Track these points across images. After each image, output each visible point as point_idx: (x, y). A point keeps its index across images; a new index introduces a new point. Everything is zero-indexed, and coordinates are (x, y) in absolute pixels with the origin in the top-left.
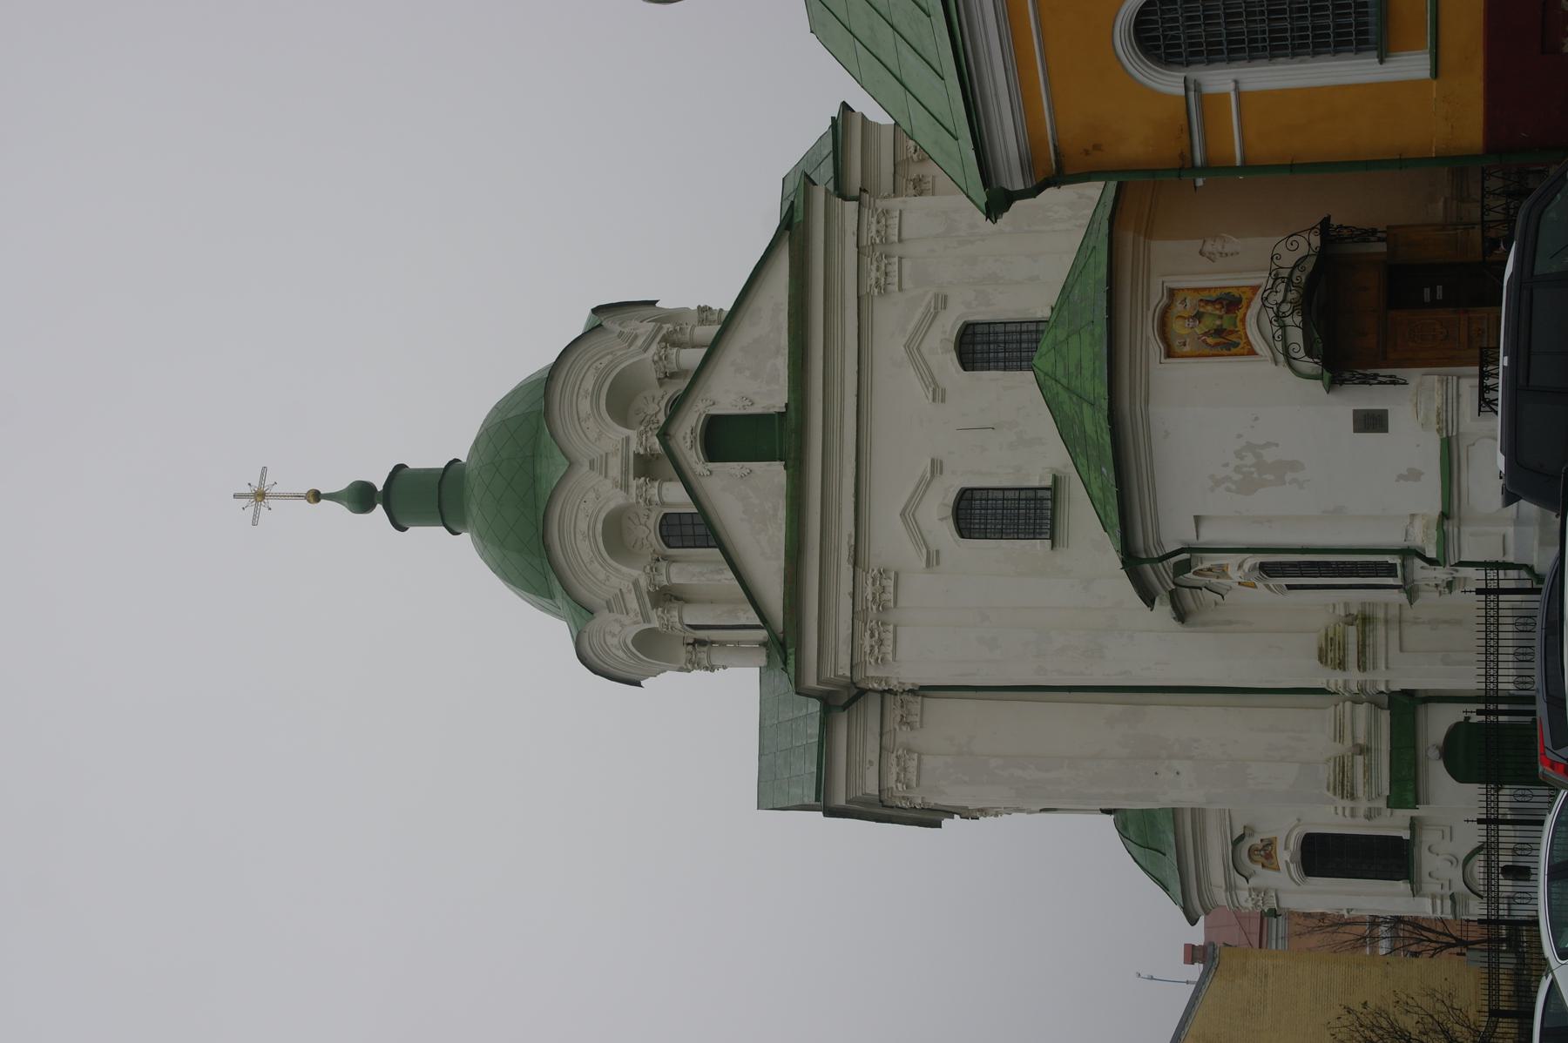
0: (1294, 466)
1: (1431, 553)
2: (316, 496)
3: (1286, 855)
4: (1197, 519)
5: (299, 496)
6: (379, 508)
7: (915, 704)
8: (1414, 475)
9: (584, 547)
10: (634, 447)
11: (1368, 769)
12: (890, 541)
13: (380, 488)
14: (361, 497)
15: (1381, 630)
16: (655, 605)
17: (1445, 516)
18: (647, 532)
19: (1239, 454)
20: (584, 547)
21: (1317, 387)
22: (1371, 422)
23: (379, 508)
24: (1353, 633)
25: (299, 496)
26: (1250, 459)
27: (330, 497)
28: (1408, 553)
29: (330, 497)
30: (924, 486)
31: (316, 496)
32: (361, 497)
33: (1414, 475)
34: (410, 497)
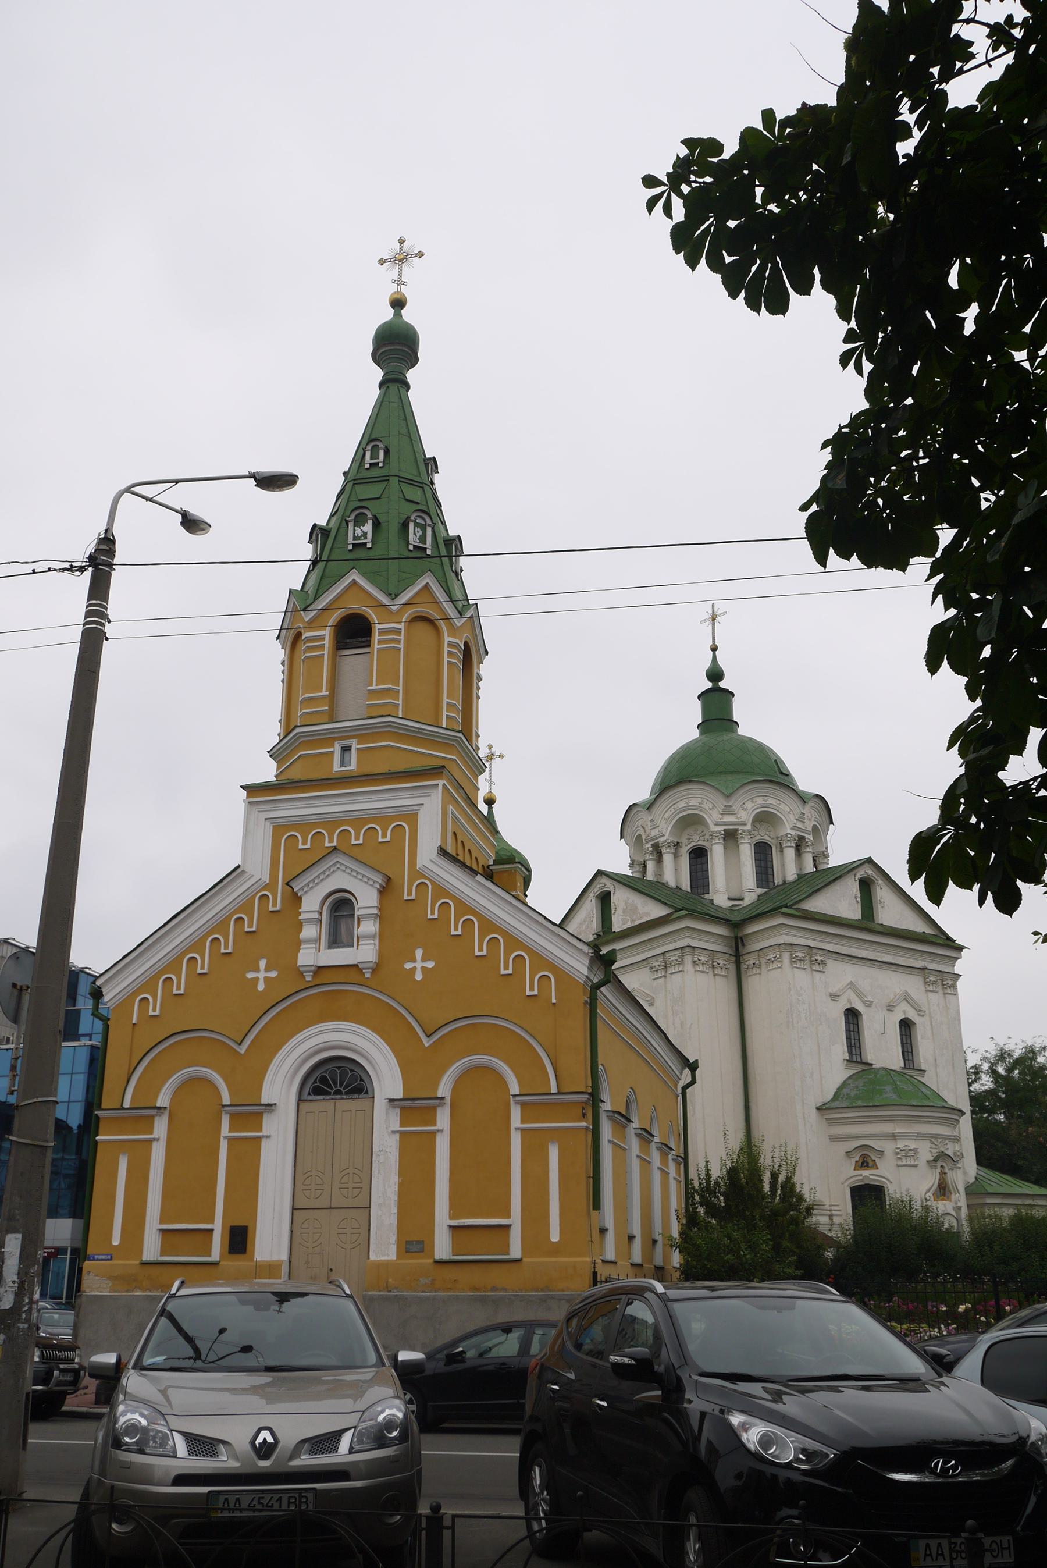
2: (714, 649)
5: (714, 639)
6: (710, 685)
9: (760, 801)
10: (807, 836)
13: (722, 684)
14: (715, 674)
16: (725, 830)
18: (764, 836)
20: (760, 801)
23: (710, 685)
25: (714, 639)
30: (860, 995)
31: (714, 649)
32: (715, 674)
34: (717, 703)
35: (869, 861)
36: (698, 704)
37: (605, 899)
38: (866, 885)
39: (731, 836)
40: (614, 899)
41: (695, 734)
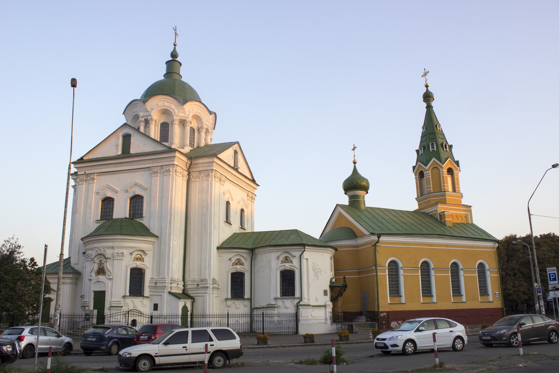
0: (318, 279)
1: (301, 303)
2: (175, 45)
3: (139, 264)
4: (307, 259)
7: (186, 179)
8: (317, 300)
11: (175, 287)
12: (228, 186)
14: (174, 55)
15: (217, 292)
16: (180, 119)
17: (313, 306)
18: (195, 125)
19: (319, 269)
21: (329, 284)
22: (325, 293)
24: (217, 286)
26: (319, 270)
27: (175, 48)
28: (301, 299)
29: (175, 48)
32: (174, 55)
33: (317, 300)
35: (238, 143)
36: (165, 66)
37: (127, 138)
38: (236, 152)
39: (183, 123)
40: (132, 140)
41: (163, 78)
